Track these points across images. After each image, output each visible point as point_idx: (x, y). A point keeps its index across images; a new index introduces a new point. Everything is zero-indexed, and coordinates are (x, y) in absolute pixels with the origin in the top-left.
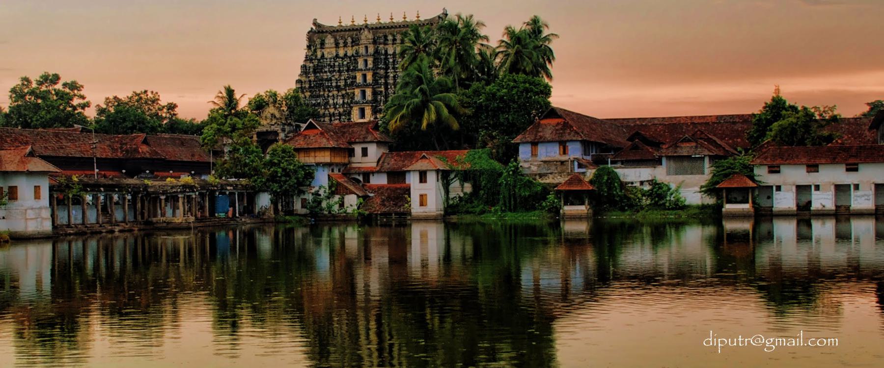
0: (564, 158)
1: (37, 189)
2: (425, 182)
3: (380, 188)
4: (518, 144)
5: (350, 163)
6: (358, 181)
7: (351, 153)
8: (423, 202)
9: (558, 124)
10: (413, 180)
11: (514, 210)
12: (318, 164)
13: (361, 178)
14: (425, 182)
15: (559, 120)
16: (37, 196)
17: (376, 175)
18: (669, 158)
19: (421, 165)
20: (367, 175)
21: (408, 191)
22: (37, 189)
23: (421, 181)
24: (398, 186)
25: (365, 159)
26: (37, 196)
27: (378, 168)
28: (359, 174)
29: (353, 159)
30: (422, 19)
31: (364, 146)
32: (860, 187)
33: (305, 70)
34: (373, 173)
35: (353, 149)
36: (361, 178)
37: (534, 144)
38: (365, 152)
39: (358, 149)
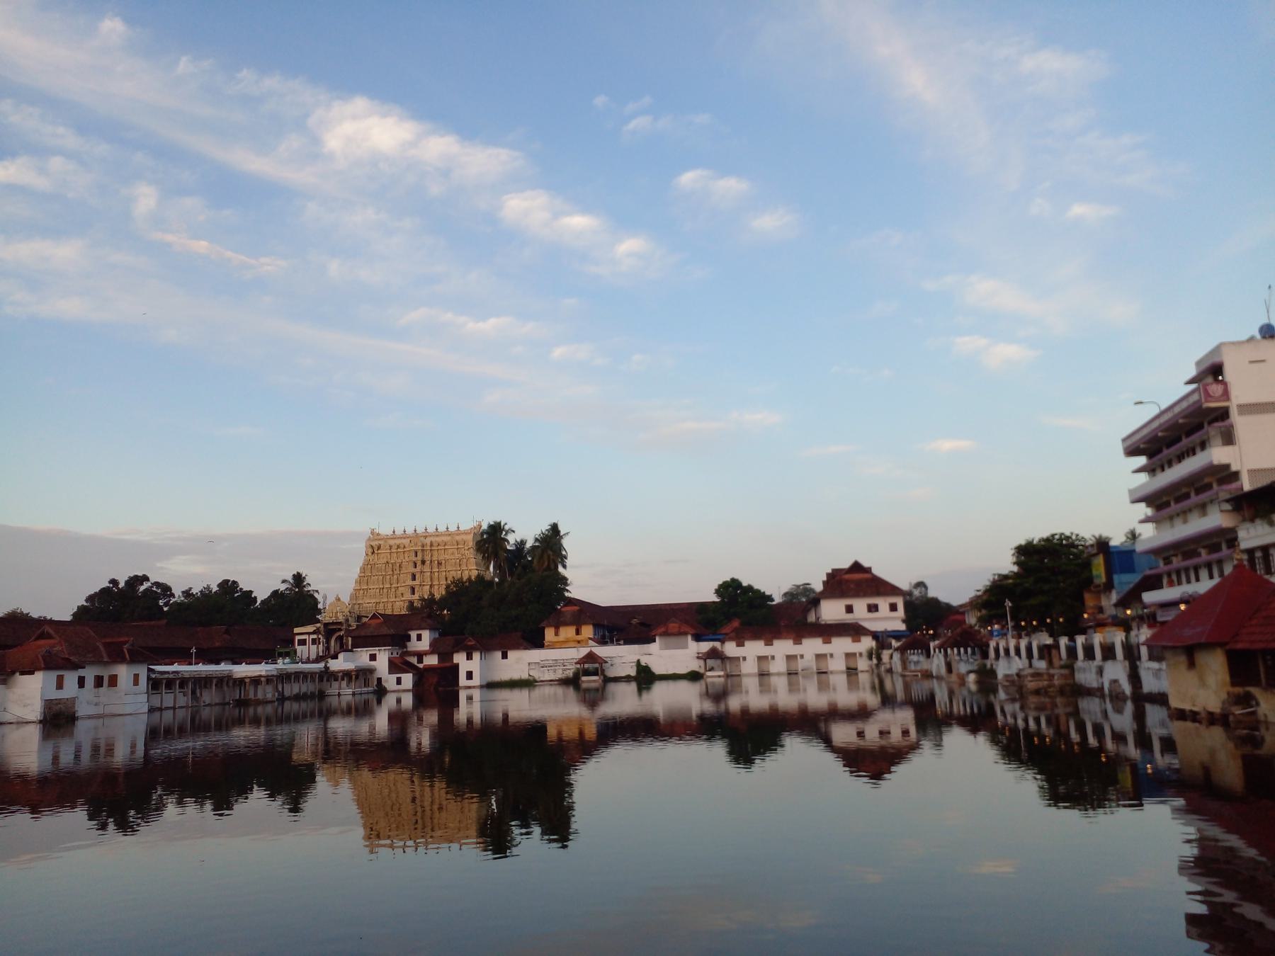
0: (579, 637)
1: (136, 677)
7: (408, 638)
8: (470, 675)
11: (1076, 658)
15: (576, 608)
16: (136, 682)
18: (661, 635)
20: (420, 656)
21: (457, 666)
22: (136, 677)
24: (448, 664)
26: (136, 682)
33: (363, 570)
34: (426, 653)
37: (557, 628)
38: (419, 638)
39: (413, 634)
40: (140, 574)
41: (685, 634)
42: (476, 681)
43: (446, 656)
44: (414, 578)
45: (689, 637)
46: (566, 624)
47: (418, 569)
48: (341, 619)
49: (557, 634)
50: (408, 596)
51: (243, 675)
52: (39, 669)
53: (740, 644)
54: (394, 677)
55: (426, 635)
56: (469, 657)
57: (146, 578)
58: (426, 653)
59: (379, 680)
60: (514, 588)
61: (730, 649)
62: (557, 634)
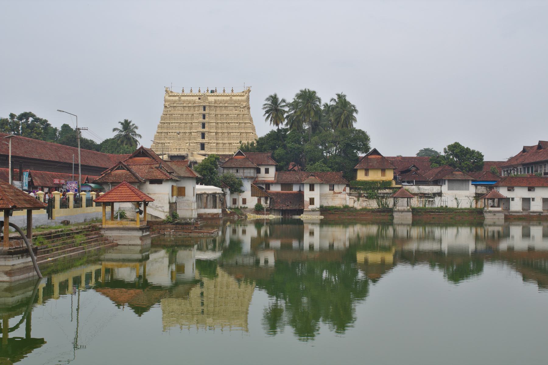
2: (313, 190)
3: (277, 194)
4: (356, 171)
5: (257, 177)
6: (263, 188)
7: (258, 171)
8: (312, 201)
9: (378, 159)
10: (306, 189)
12: (246, 178)
13: (264, 187)
14: (313, 190)
17: (274, 185)
18: (449, 181)
19: (312, 179)
21: (301, 194)
23: (310, 190)
25: (267, 175)
27: (276, 181)
28: (263, 184)
29: (259, 175)
30: (235, 93)
31: (267, 167)
32: (535, 200)
35: (260, 169)
36: (264, 187)
38: (267, 171)
39: (263, 170)
40: (28, 111)
41: (467, 181)
42: (317, 205)
43: (286, 185)
44: (204, 127)
45: (470, 183)
46: (374, 168)
47: (207, 120)
48: (183, 153)
49: (366, 174)
50: (201, 140)
51: (203, 192)
52: (167, 180)
53: (510, 189)
54: (256, 199)
55: (272, 170)
56: (312, 189)
57: (33, 116)
58: (272, 183)
59: (244, 201)
60: (316, 138)
61: (503, 192)
62: (366, 174)
